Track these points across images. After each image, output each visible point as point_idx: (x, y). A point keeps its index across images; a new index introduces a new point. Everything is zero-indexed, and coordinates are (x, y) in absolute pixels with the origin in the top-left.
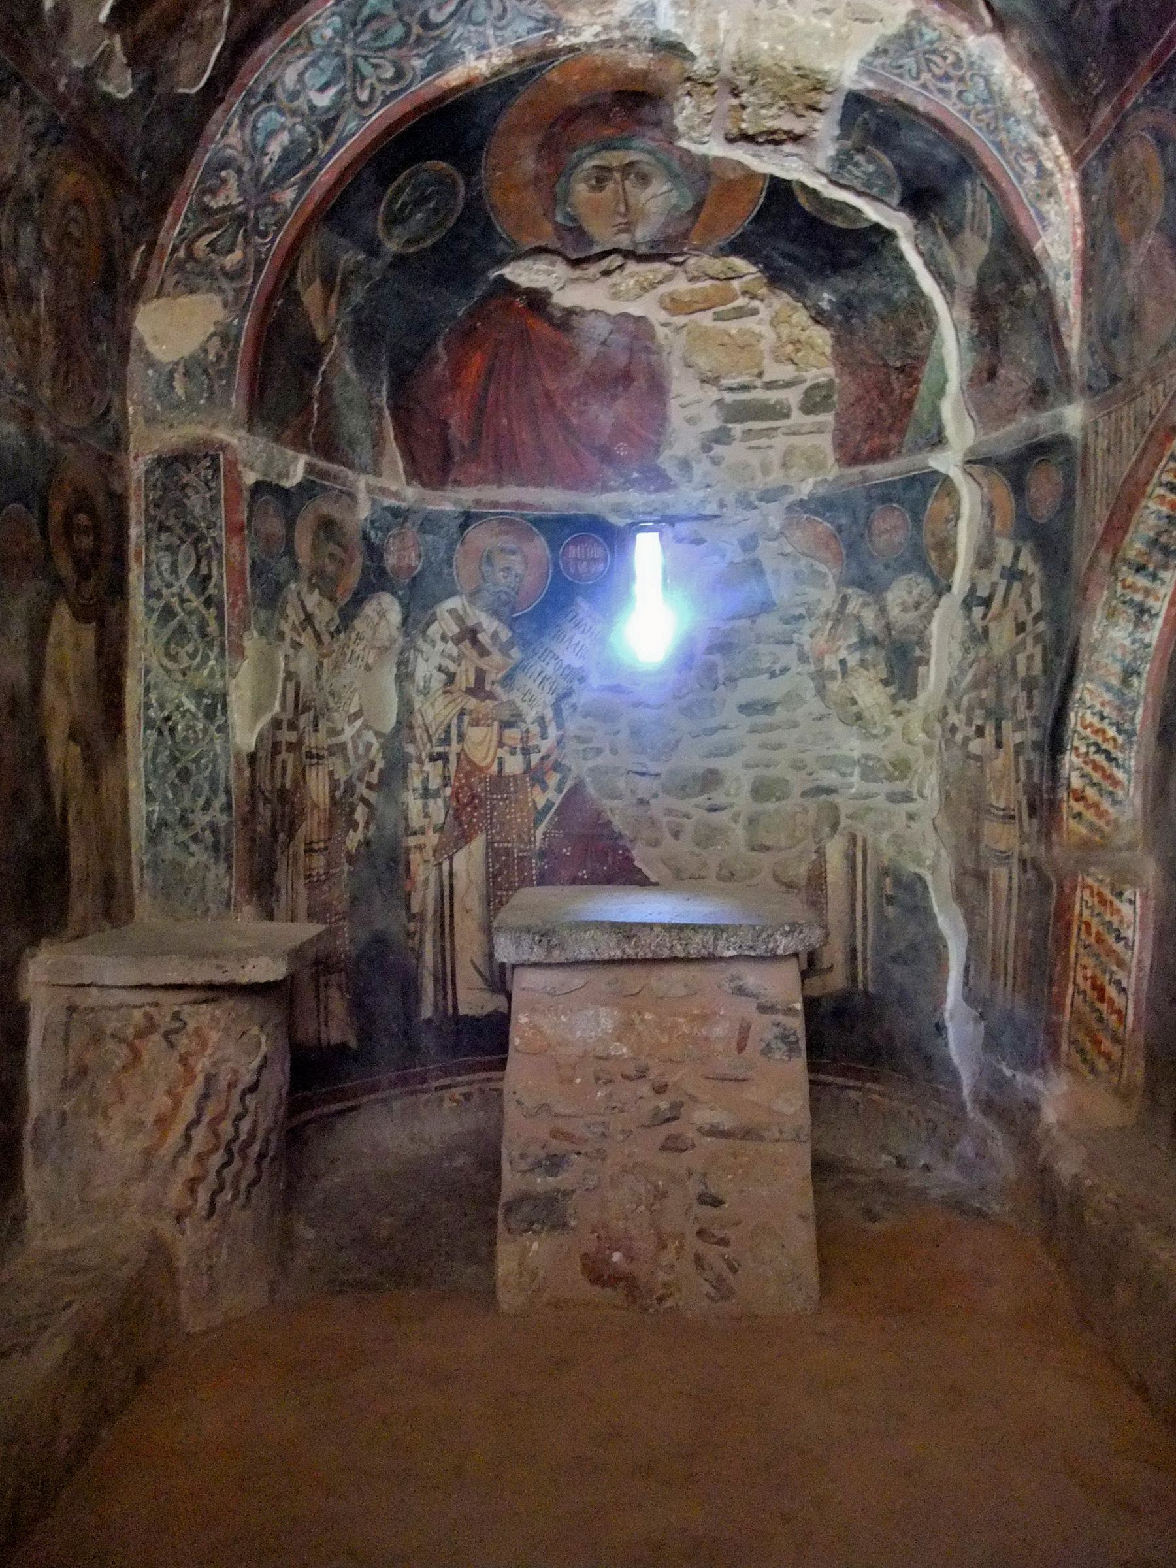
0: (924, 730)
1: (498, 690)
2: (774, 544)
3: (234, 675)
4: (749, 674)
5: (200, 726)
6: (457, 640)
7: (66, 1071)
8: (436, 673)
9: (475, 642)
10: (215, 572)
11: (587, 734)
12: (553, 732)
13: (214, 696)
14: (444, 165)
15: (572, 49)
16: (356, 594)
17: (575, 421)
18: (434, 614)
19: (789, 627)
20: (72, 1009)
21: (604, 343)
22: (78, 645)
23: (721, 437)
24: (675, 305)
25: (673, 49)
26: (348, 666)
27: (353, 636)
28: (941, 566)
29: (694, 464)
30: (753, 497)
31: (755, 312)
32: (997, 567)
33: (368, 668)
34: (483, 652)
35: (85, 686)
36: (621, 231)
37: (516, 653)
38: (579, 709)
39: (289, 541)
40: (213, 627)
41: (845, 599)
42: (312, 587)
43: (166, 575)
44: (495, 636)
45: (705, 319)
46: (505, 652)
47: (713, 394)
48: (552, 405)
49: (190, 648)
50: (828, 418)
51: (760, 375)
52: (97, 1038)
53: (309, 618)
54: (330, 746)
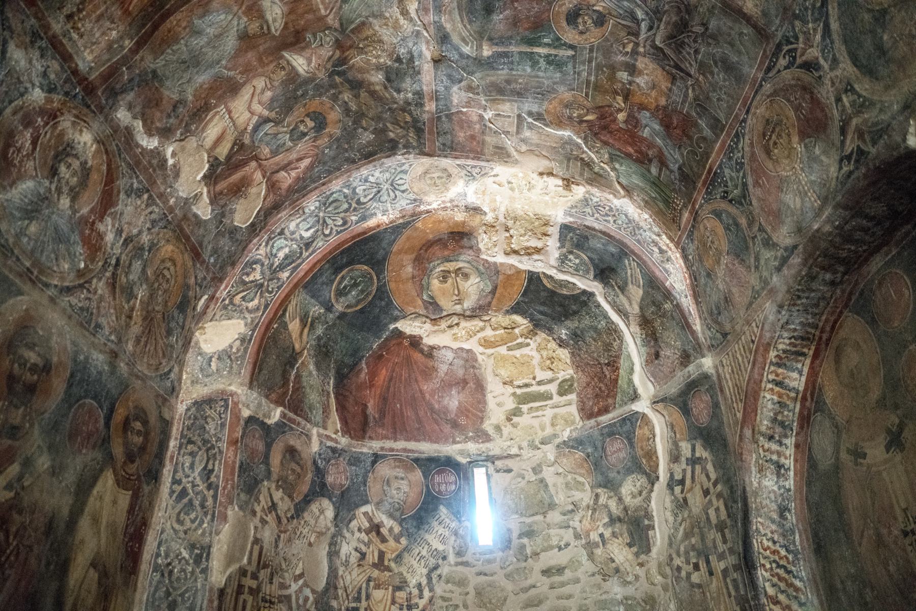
0: (660, 574)
1: (393, 565)
2: (552, 469)
3: (218, 533)
4: (545, 550)
5: (190, 569)
6: (368, 532)
8: (353, 552)
9: (378, 533)
10: (216, 468)
11: (447, 595)
12: (427, 594)
13: (202, 548)
14: (366, 267)
15: (428, 212)
16: (306, 496)
17: (437, 406)
18: (355, 514)
19: (566, 517)
21: (450, 364)
22: (115, 502)
23: (517, 412)
24: (487, 343)
25: (476, 210)
26: (297, 542)
27: (303, 522)
28: (650, 466)
29: (503, 428)
30: (537, 443)
31: (528, 345)
32: (683, 459)
33: (310, 544)
34: (384, 540)
35: (114, 534)
36: (456, 304)
37: (404, 541)
38: (443, 578)
39: (267, 456)
40: (210, 502)
41: (597, 496)
42: (277, 488)
43: (186, 469)
44: (391, 530)
45: (503, 350)
46: (397, 540)
47: (510, 390)
48: (424, 398)
49: (193, 516)
50: (573, 397)
51: (534, 378)
53: (273, 507)
54: (281, 596)
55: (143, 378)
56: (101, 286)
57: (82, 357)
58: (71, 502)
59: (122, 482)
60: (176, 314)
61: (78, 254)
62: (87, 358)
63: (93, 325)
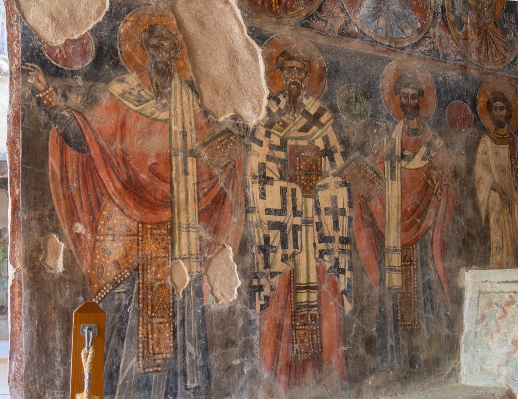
7: (477, 316)
20: (480, 292)
22: (497, 154)
35: (503, 171)
52: (490, 304)
55: (494, 73)
56: (437, 31)
57: (441, 79)
58: (464, 159)
59: (498, 141)
60: (506, 16)
61: (414, 20)
62: (444, 78)
63: (441, 57)
